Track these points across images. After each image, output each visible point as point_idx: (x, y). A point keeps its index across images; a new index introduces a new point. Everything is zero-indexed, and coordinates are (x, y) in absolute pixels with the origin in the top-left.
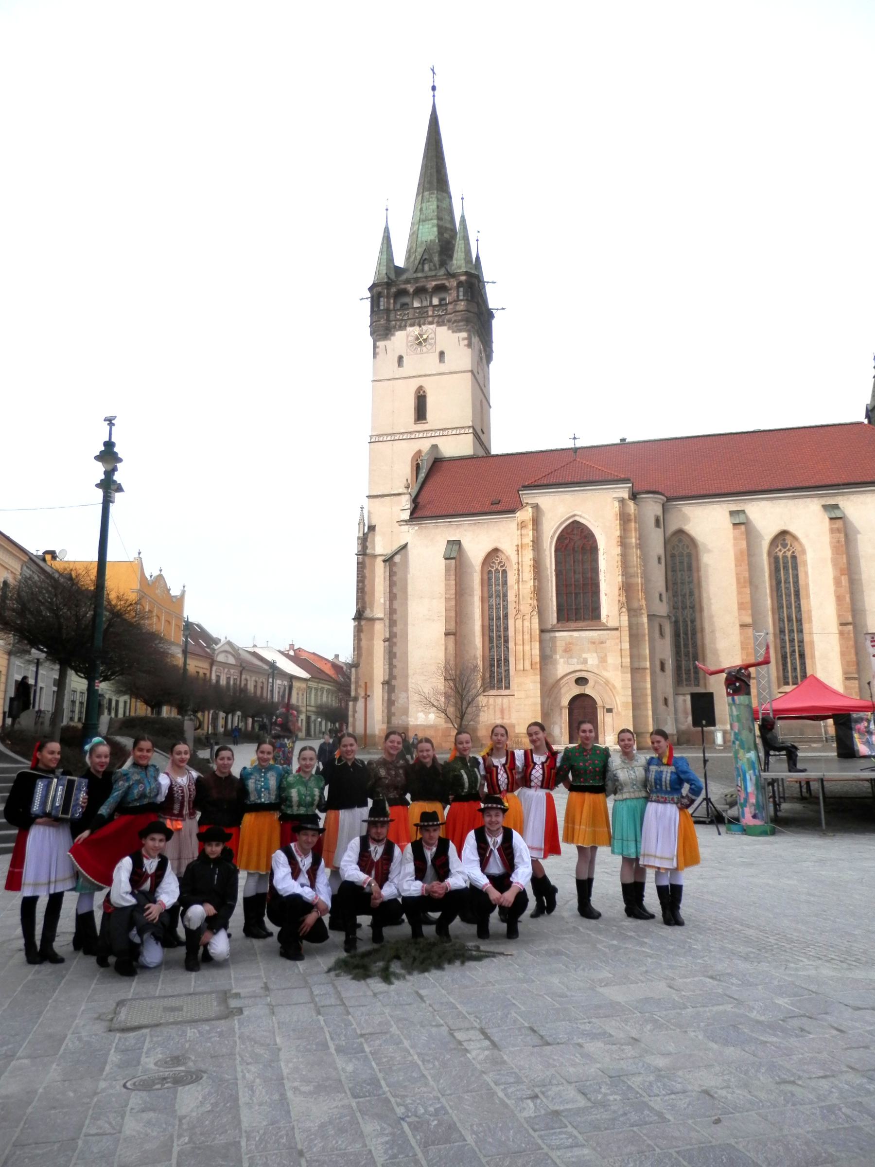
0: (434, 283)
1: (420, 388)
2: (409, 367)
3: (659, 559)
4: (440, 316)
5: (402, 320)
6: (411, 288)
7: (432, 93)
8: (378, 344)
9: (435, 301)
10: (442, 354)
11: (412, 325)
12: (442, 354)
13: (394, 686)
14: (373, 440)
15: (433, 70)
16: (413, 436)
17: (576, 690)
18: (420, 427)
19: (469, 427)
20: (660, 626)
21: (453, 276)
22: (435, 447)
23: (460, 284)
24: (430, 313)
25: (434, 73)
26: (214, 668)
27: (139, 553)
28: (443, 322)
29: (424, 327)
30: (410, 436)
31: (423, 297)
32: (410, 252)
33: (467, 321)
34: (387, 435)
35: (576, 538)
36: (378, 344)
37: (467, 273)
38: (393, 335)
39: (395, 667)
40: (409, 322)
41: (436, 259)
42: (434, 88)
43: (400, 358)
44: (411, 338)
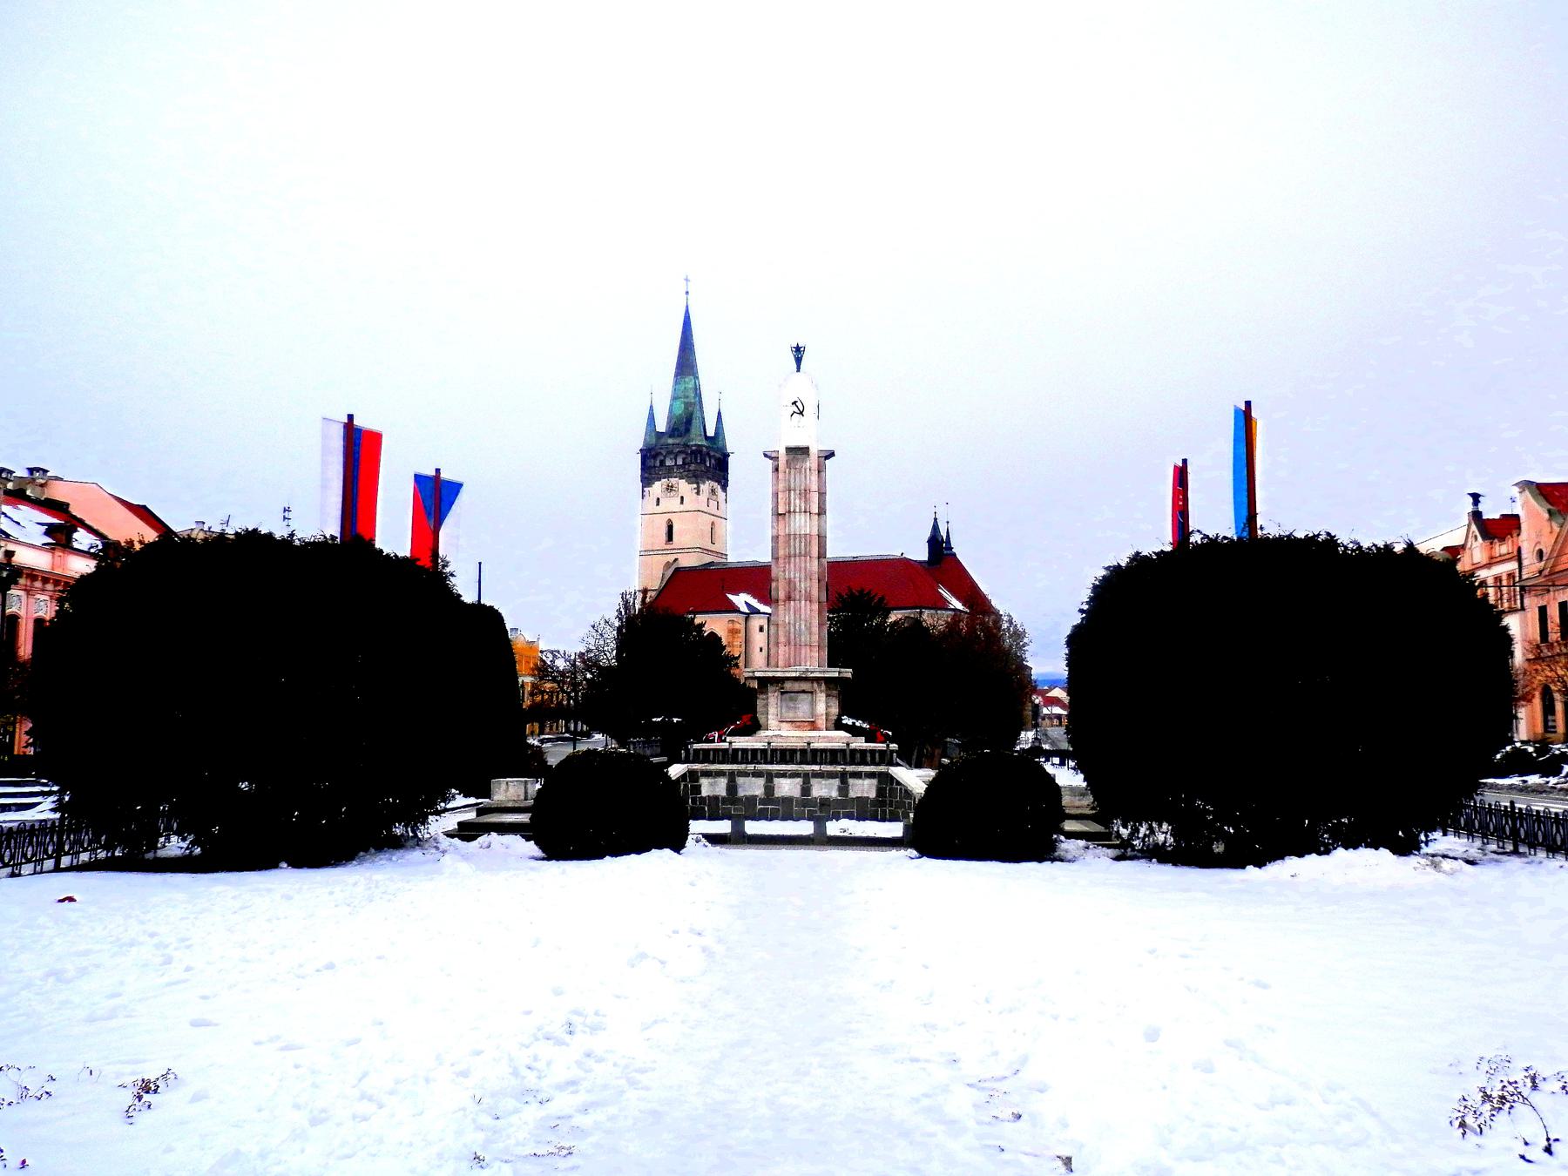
1: (670, 520)
3: (761, 650)
4: (681, 473)
8: (645, 489)
9: (680, 462)
10: (682, 498)
12: (682, 498)
18: (668, 547)
22: (676, 559)
23: (693, 452)
25: (687, 280)
31: (672, 457)
32: (670, 419)
36: (645, 489)
37: (695, 445)
41: (682, 429)
42: (687, 293)
43: (658, 499)
44: (664, 486)
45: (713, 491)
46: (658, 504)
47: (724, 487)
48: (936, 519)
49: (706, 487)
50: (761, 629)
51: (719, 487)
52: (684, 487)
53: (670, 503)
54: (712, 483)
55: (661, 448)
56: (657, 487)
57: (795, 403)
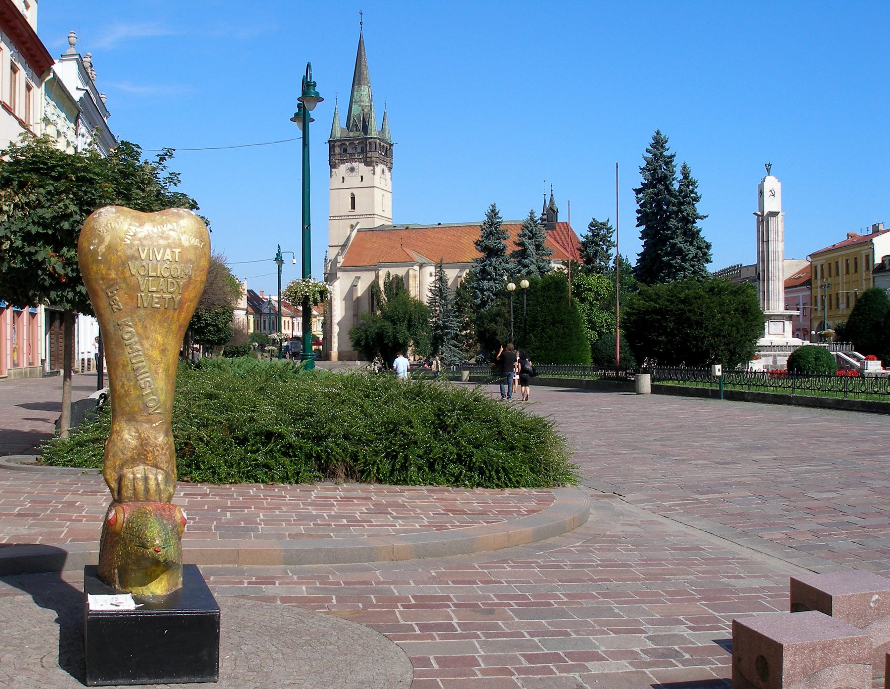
1: (352, 194)
6: (347, 143)
8: (333, 170)
14: (332, 218)
15: (361, 14)
16: (349, 217)
24: (356, 156)
25: (361, 14)
26: (262, 317)
29: (353, 163)
30: (346, 218)
34: (337, 216)
36: (333, 170)
37: (371, 138)
38: (339, 166)
43: (343, 178)
45: (383, 172)
48: (552, 195)
52: (361, 167)
53: (353, 181)
57: (771, 191)
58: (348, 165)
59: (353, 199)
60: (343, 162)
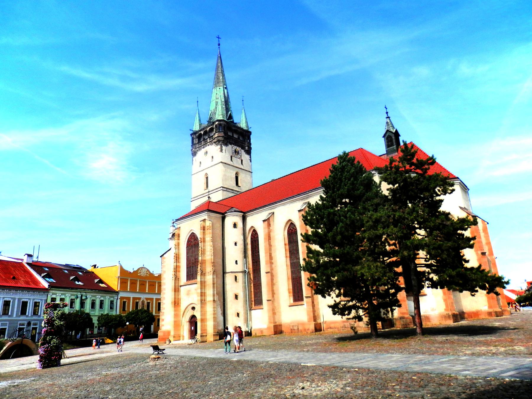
0: (209, 128)
1: (206, 174)
2: (203, 166)
3: (236, 244)
4: (211, 141)
5: (200, 147)
7: (218, 46)
10: (213, 157)
11: (204, 148)
13: (164, 312)
17: (190, 313)
19: (221, 187)
20: (236, 277)
21: (214, 123)
24: (208, 141)
25: (219, 38)
27: (119, 262)
28: (212, 144)
33: (219, 141)
35: (192, 240)
37: (218, 121)
39: (164, 303)
40: (202, 147)
42: (219, 45)
43: (200, 163)
46: (200, 166)
47: (249, 152)
49: (229, 149)
50: (235, 226)
51: (243, 151)
54: (235, 147)
55: (201, 130)
56: (201, 153)
58: (203, 150)
59: (207, 178)
60: (200, 149)
